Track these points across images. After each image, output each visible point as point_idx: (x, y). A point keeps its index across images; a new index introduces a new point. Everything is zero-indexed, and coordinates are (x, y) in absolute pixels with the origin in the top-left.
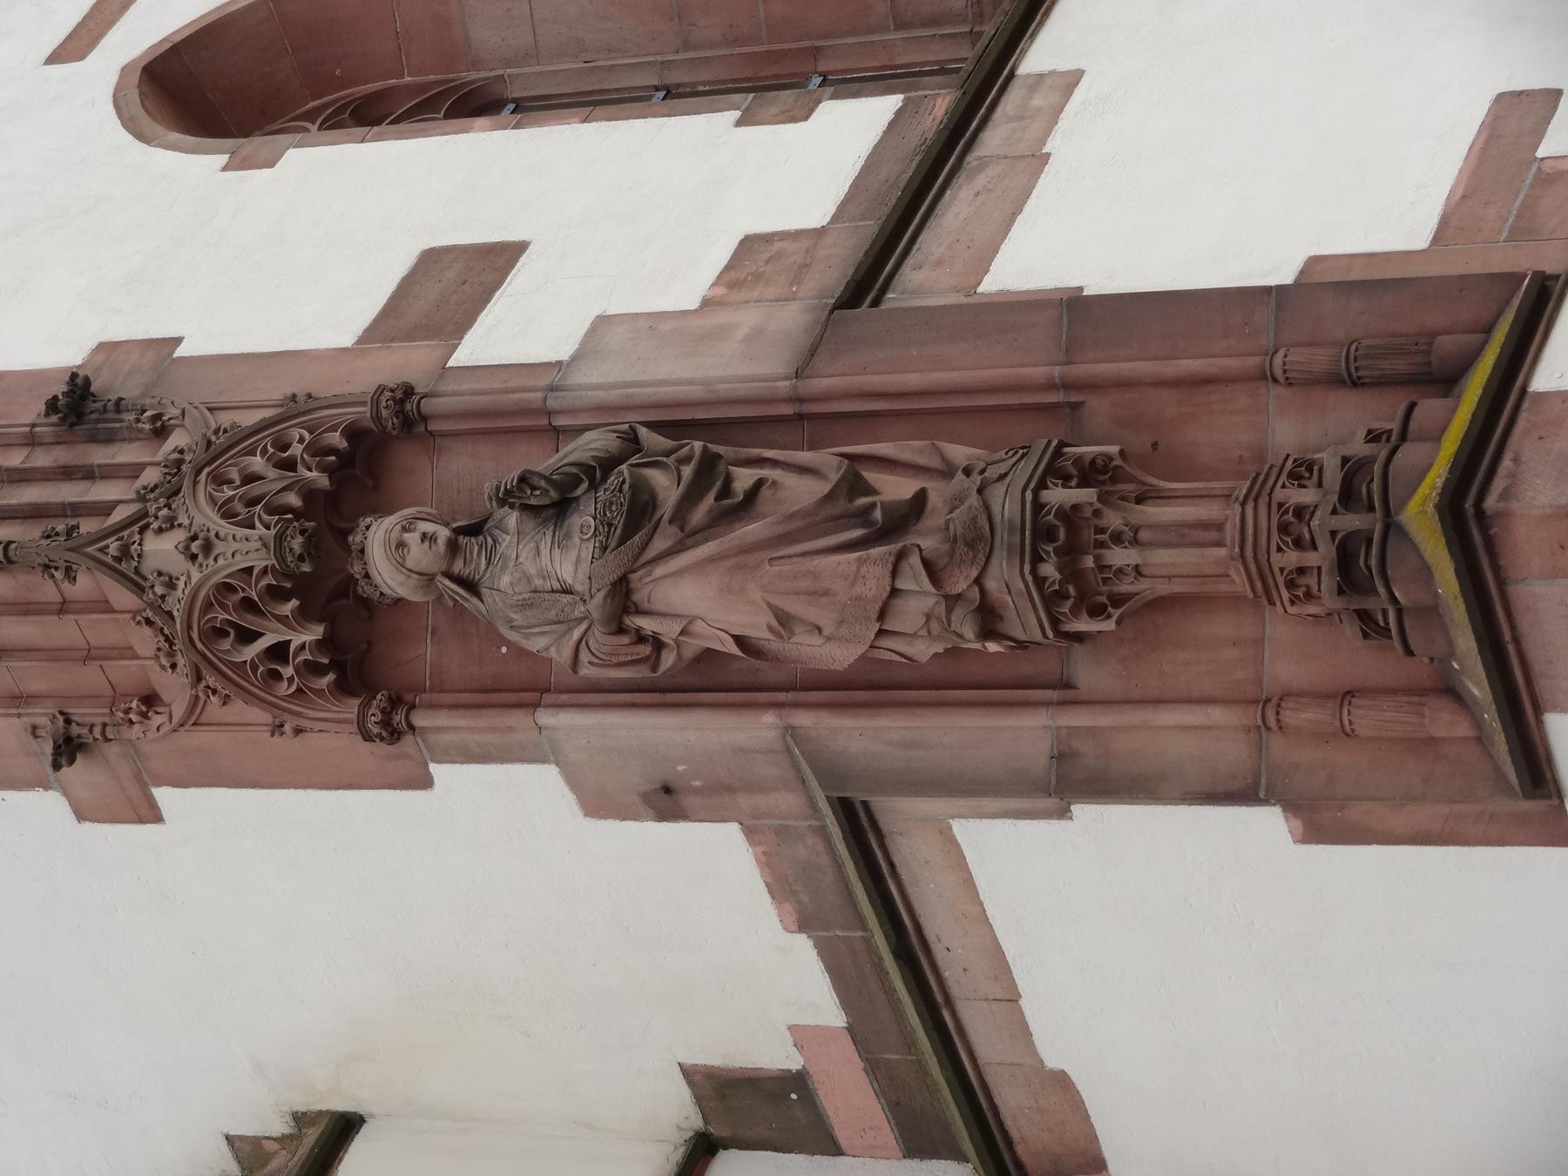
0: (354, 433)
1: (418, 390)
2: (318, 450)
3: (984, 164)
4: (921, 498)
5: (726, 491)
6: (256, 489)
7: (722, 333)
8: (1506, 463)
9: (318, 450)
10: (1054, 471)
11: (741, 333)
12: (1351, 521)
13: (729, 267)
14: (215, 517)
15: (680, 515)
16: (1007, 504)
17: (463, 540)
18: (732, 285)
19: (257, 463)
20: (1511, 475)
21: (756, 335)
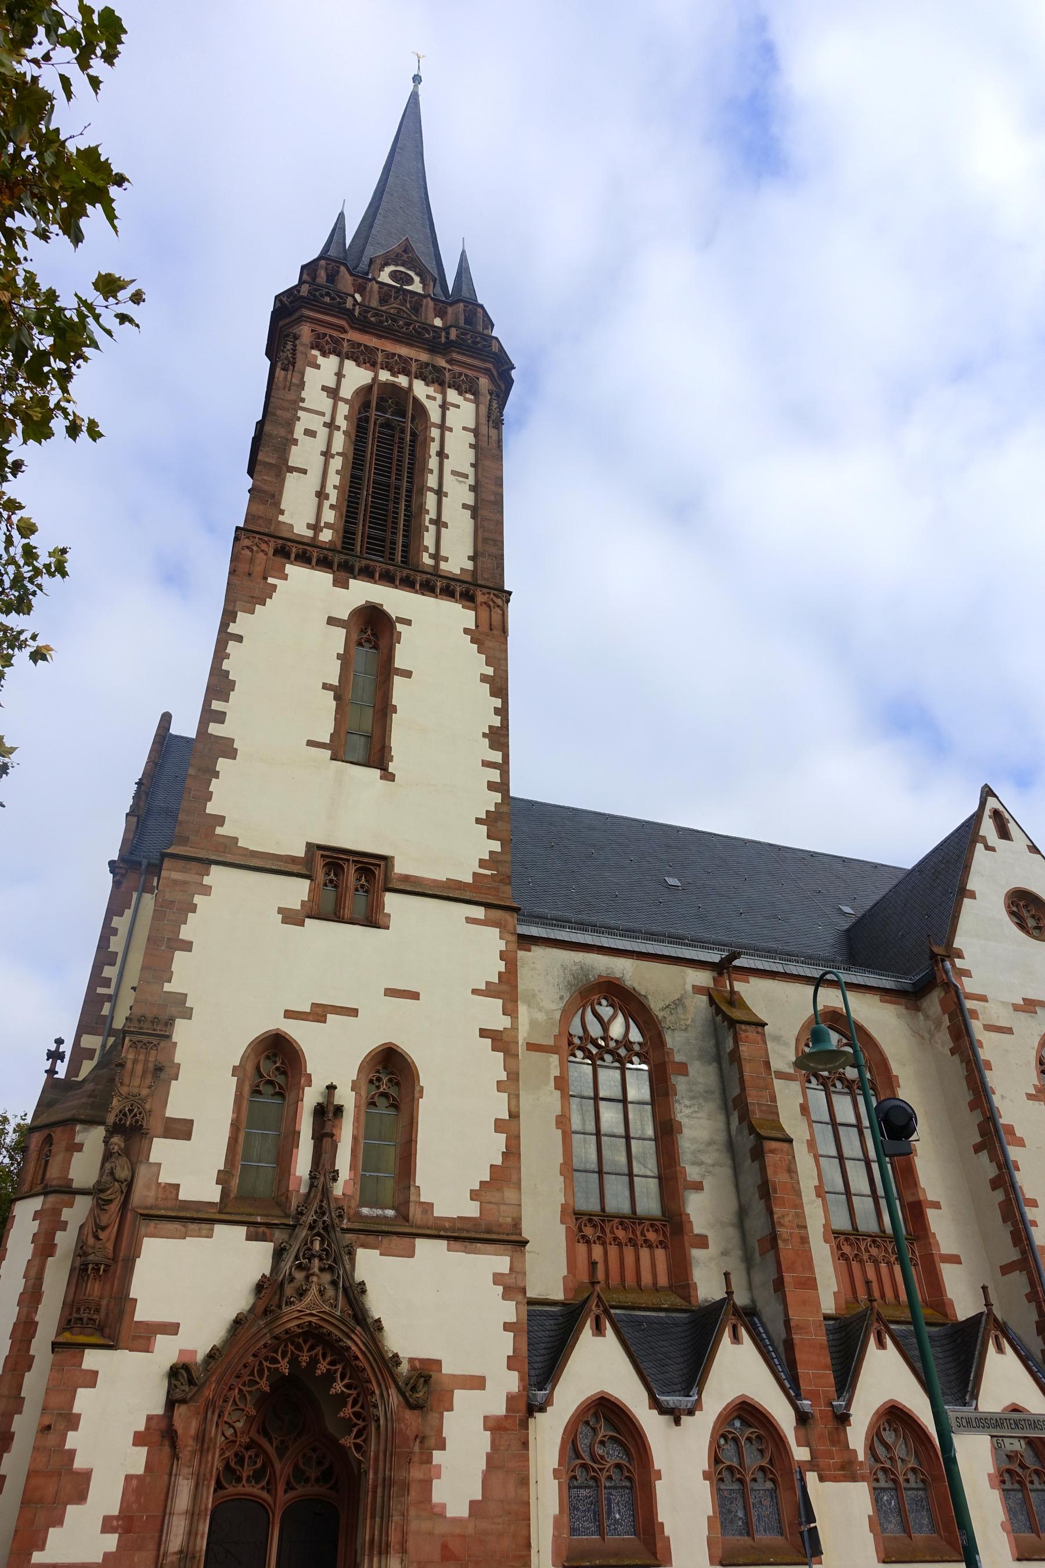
0: (142, 1126)
1: (148, 1136)
2: (137, 1121)
3: (185, 1226)
4: (101, 1240)
5: (104, 1205)
6: (128, 1114)
7: (149, 1188)
8: (66, 1350)
9: (137, 1121)
10: (97, 1265)
11: (148, 1194)
12: (85, 1320)
13: (170, 1184)
14: (121, 1107)
15: (100, 1198)
16: (91, 1258)
17: (117, 1154)
18: (165, 1187)
19: (135, 1110)
20: (62, 1351)
21: (147, 1196)
